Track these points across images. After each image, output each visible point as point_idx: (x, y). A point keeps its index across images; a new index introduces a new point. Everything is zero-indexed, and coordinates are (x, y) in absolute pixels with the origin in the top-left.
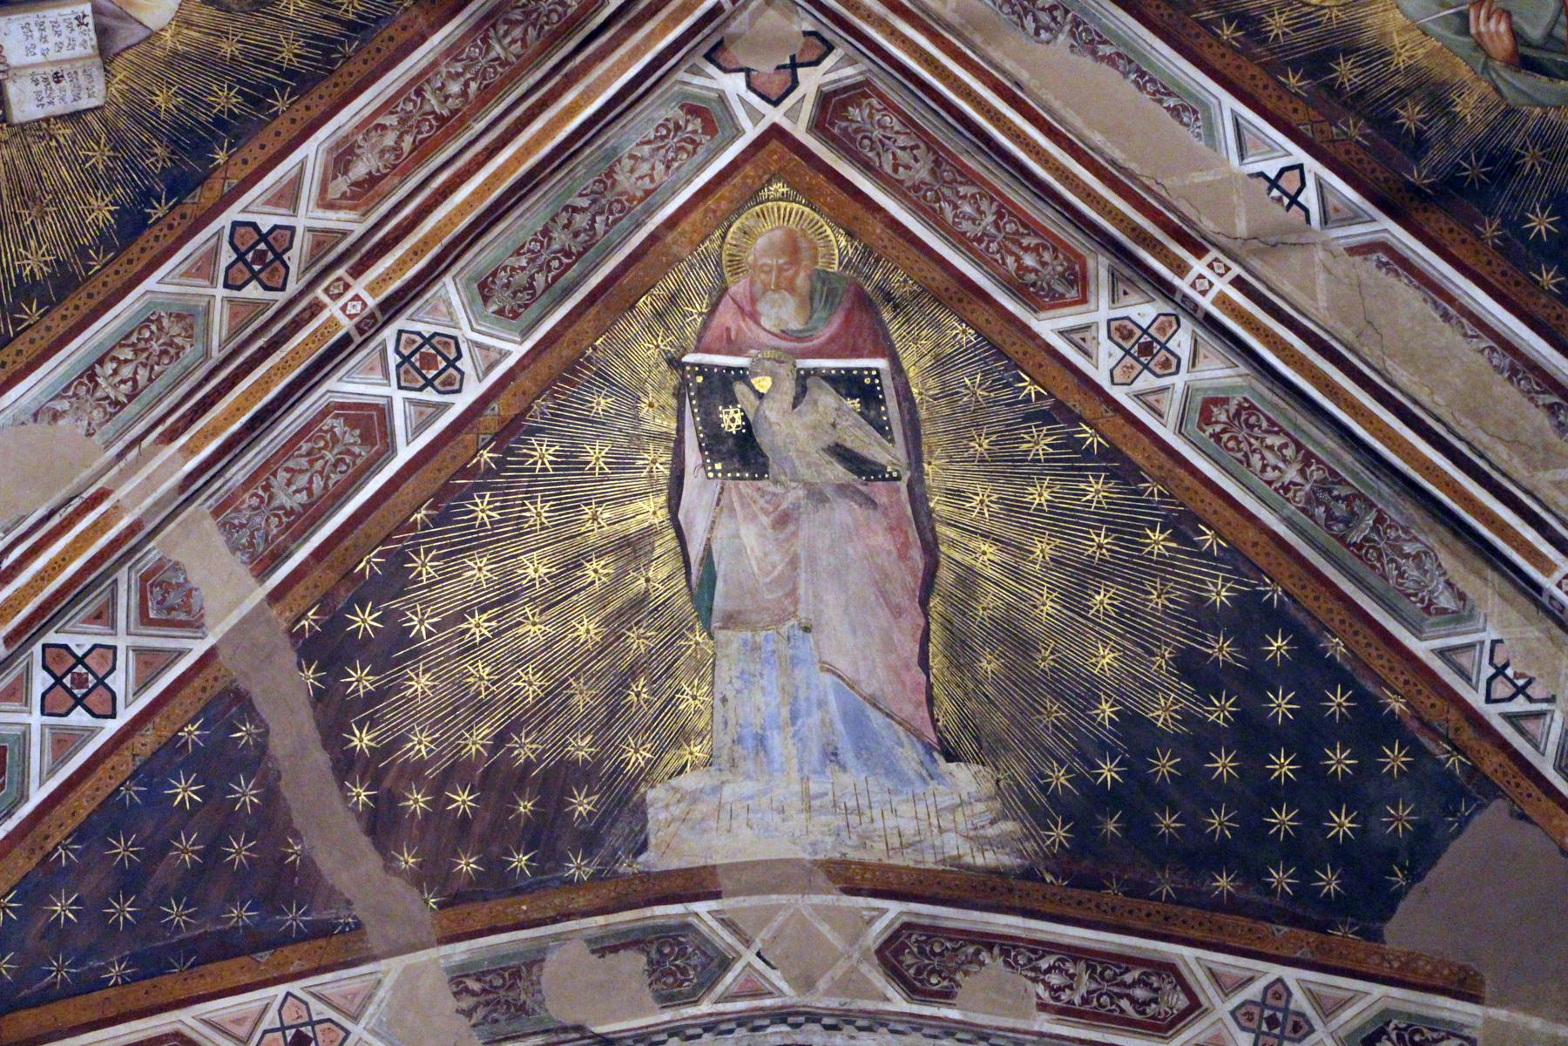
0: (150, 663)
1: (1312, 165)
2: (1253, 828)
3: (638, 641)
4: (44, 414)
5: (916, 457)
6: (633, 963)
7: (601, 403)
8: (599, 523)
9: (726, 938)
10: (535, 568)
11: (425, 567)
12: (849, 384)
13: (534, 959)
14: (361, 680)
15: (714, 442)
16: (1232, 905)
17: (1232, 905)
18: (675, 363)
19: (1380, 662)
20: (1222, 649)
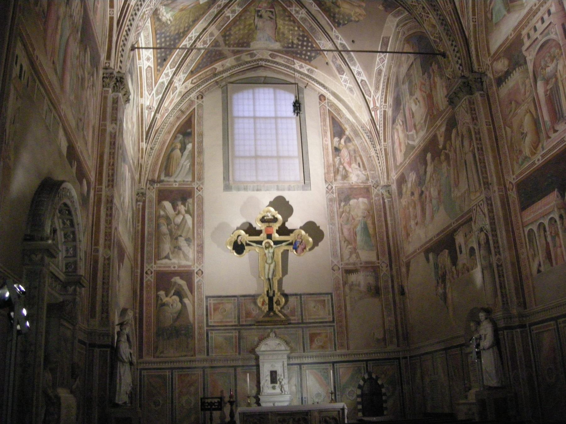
0: (210, 40)
1: (314, 3)
2: (301, 52)
3: (251, 32)
4: (202, 23)
5: (276, 18)
6: (249, 56)
7: (248, 13)
8: (248, 23)
9: (256, 53)
10: (242, 27)
11: (232, 28)
12: (270, 11)
13: (240, 57)
14: (227, 38)
15: (258, 16)
16: (299, 58)
17: (299, 58)
18: (255, 9)
19: (313, 42)
20: (301, 38)
